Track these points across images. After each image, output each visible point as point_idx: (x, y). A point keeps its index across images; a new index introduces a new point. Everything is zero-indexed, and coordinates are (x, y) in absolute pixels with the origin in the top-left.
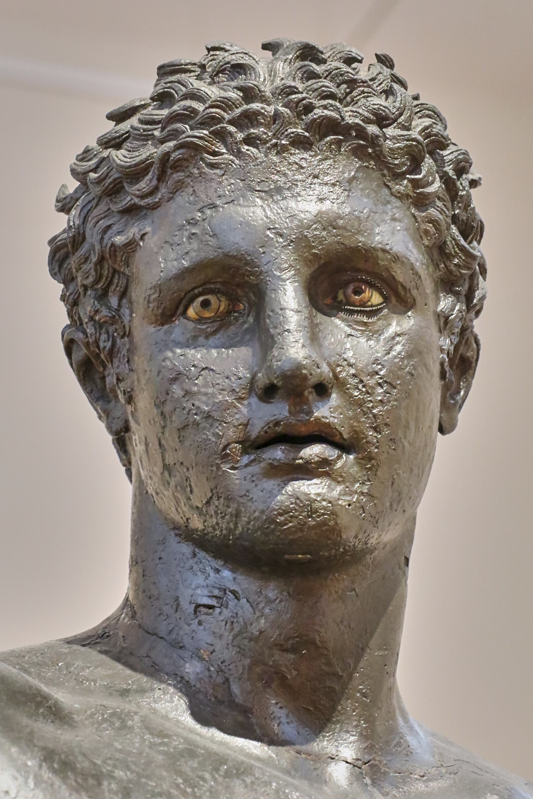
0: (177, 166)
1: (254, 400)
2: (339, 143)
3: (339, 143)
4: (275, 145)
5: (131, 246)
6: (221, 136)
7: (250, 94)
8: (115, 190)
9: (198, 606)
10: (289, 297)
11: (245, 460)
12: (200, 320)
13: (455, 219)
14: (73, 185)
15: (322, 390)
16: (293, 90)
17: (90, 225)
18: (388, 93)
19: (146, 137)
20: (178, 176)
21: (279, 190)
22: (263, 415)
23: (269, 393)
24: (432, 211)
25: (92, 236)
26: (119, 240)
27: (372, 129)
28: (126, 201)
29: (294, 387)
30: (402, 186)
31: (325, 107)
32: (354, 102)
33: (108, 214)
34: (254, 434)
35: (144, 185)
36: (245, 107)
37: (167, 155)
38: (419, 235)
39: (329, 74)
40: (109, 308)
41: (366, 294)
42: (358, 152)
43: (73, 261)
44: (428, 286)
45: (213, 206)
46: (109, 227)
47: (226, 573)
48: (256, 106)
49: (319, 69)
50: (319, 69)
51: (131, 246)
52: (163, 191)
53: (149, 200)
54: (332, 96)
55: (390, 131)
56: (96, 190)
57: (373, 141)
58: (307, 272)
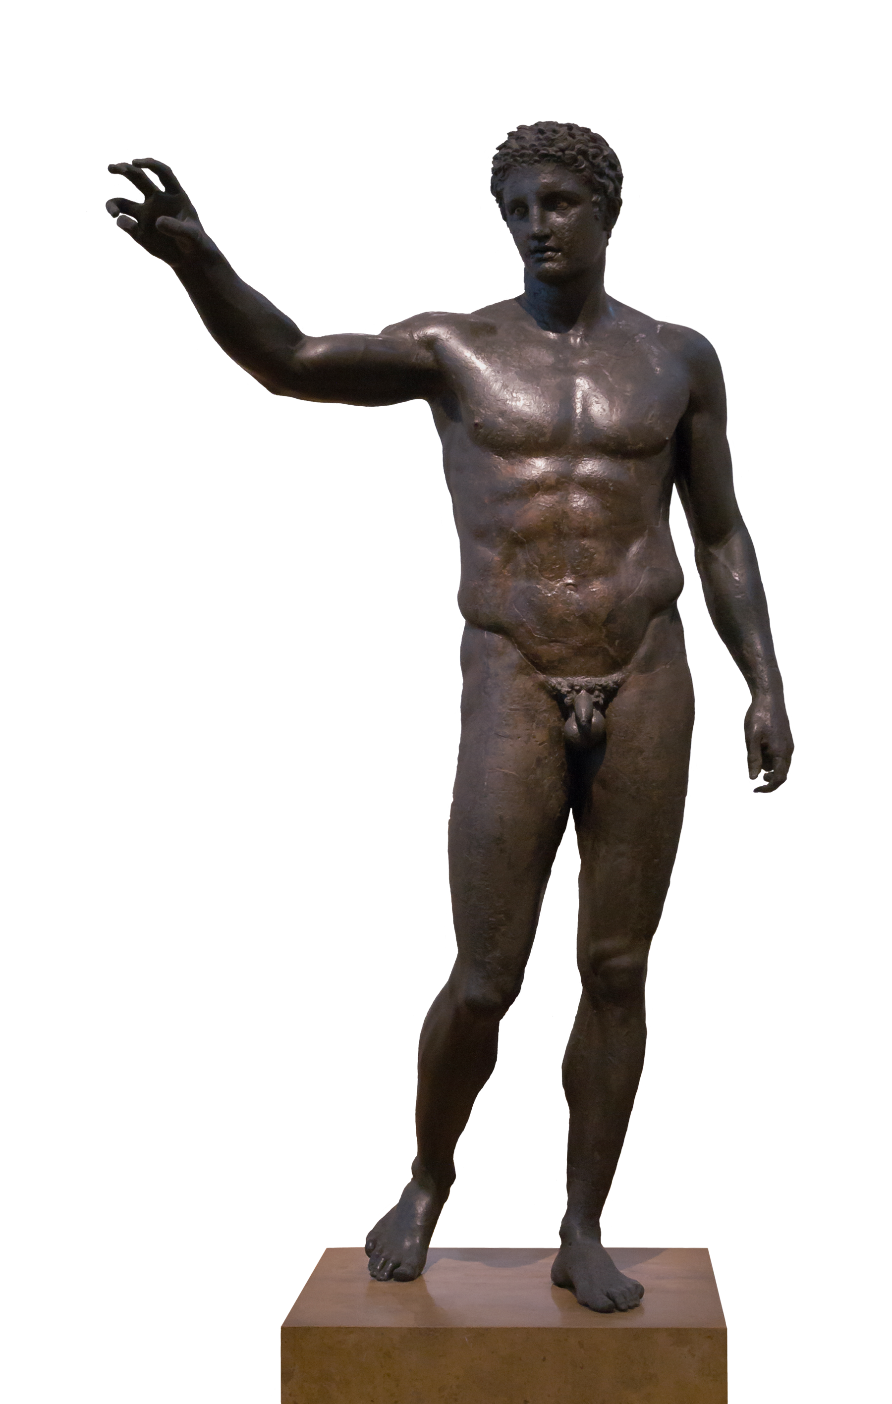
7: (523, 148)
10: (535, 211)
16: (534, 145)
22: (534, 244)
24: (585, 173)
26: (499, 189)
27: (560, 154)
32: (554, 145)
42: (554, 161)
51: (502, 190)
54: (545, 146)
55: (567, 152)
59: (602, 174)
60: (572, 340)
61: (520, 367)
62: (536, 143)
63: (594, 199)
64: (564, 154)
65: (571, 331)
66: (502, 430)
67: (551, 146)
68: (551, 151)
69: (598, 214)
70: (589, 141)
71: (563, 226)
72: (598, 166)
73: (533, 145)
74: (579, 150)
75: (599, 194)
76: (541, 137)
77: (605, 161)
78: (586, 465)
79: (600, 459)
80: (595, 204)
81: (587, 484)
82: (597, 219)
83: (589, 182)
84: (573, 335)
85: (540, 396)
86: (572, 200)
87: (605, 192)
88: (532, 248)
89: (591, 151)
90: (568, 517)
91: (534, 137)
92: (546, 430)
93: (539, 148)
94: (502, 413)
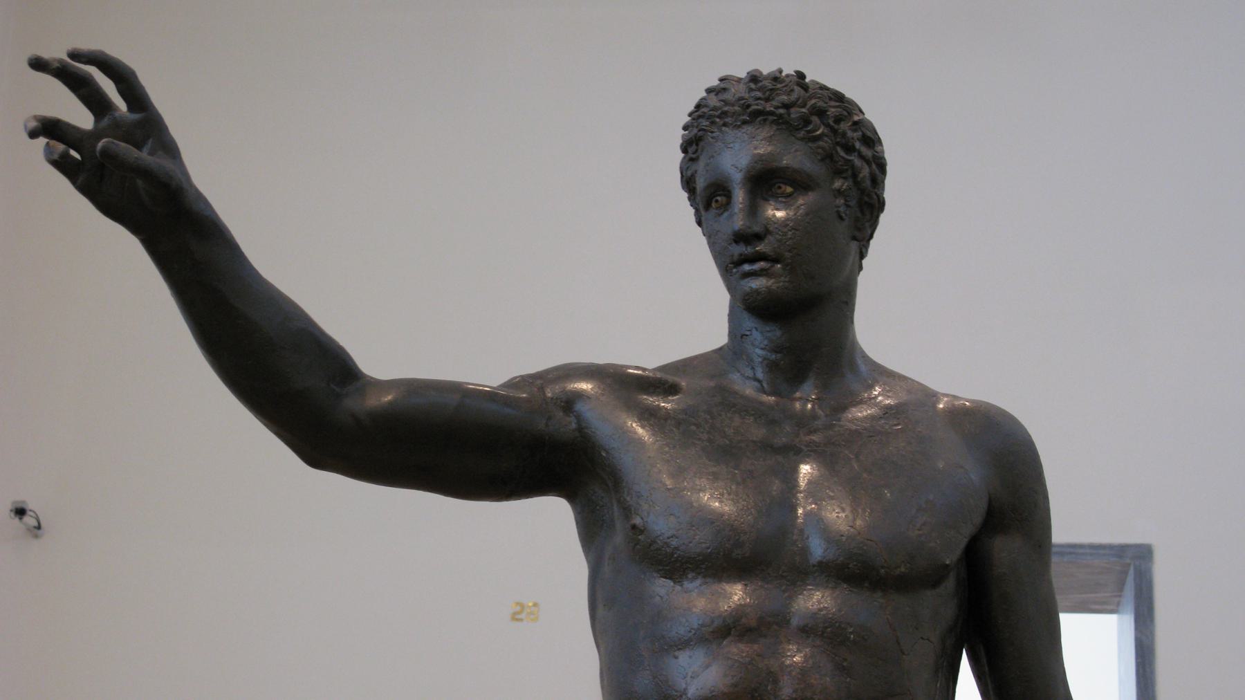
3: (765, 120)
6: (713, 123)
7: (726, 103)
13: (838, 144)
22: (739, 250)
27: (782, 111)
30: (802, 134)
42: (773, 122)
55: (792, 110)
59: (849, 149)
60: (798, 405)
61: (710, 440)
62: (747, 96)
63: (837, 184)
64: (789, 115)
65: (798, 395)
67: (767, 100)
68: (769, 108)
69: (842, 209)
70: (831, 99)
71: (784, 223)
72: (844, 135)
73: (741, 99)
74: (813, 107)
75: (845, 178)
76: (753, 86)
77: (855, 131)
78: (810, 597)
79: (834, 588)
80: (839, 193)
81: (810, 630)
82: (841, 218)
83: (828, 157)
84: (800, 399)
85: (738, 484)
86: (801, 183)
87: (855, 176)
88: (736, 258)
89: (832, 112)
90: (776, 682)
91: (742, 87)
93: (751, 101)
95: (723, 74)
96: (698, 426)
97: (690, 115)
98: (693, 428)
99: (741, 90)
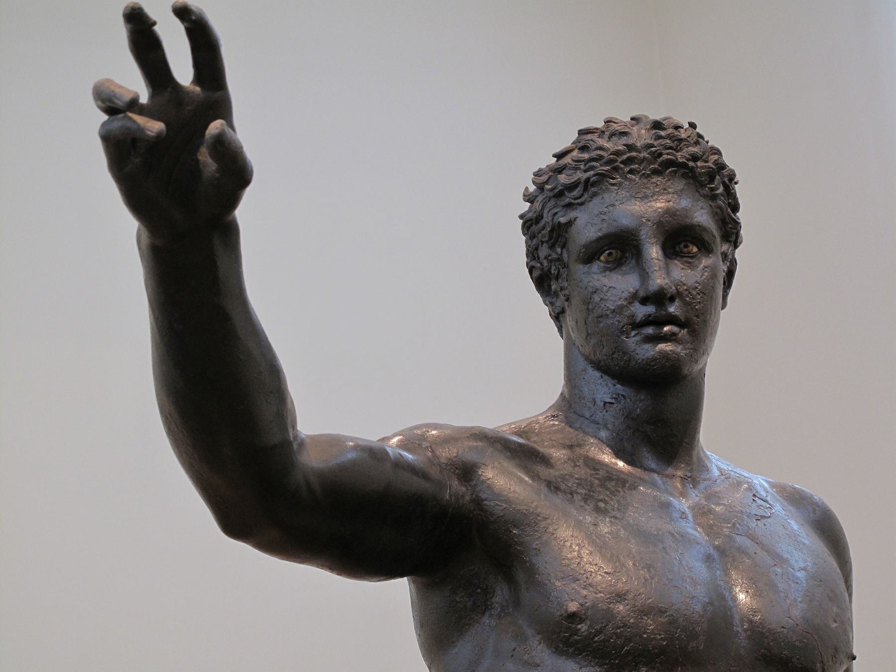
0: (594, 184)
1: (637, 304)
2: (675, 172)
4: (644, 174)
5: (570, 223)
6: (616, 169)
7: (630, 147)
8: (560, 195)
9: (605, 403)
10: (654, 252)
11: (633, 333)
12: (607, 262)
14: (532, 188)
15: (672, 299)
16: (652, 146)
17: (546, 211)
18: (697, 143)
19: (576, 169)
20: (593, 189)
21: (646, 197)
22: (641, 311)
23: (644, 301)
25: (547, 218)
26: (563, 220)
27: (691, 164)
28: (567, 200)
29: (659, 298)
30: (706, 191)
31: (668, 154)
33: (555, 206)
34: (638, 320)
35: (575, 193)
36: (628, 155)
37: (588, 179)
38: (714, 214)
39: (669, 137)
40: (557, 253)
41: (691, 248)
42: (684, 176)
43: (534, 228)
44: (718, 240)
45: (613, 205)
46: (556, 213)
47: (618, 386)
48: (634, 154)
49: (663, 133)
50: (663, 133)
51: (570, 223)
52: (586, 196)
53: (579, 201)
54: (671, 148)
55: (699, 164)
56: (547, 194)
57: (692, 169)
58: (662, 239)
66: (625, 625)
68: (680, 157)
92: (698, 629)
94: (620, 597)
95: (635, 114)
96: (606, 503)
97: (559, 156)
98: (601, 505)
99: (641, 136)
